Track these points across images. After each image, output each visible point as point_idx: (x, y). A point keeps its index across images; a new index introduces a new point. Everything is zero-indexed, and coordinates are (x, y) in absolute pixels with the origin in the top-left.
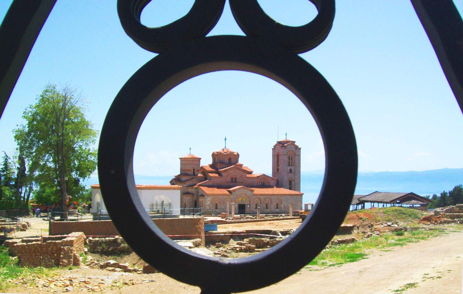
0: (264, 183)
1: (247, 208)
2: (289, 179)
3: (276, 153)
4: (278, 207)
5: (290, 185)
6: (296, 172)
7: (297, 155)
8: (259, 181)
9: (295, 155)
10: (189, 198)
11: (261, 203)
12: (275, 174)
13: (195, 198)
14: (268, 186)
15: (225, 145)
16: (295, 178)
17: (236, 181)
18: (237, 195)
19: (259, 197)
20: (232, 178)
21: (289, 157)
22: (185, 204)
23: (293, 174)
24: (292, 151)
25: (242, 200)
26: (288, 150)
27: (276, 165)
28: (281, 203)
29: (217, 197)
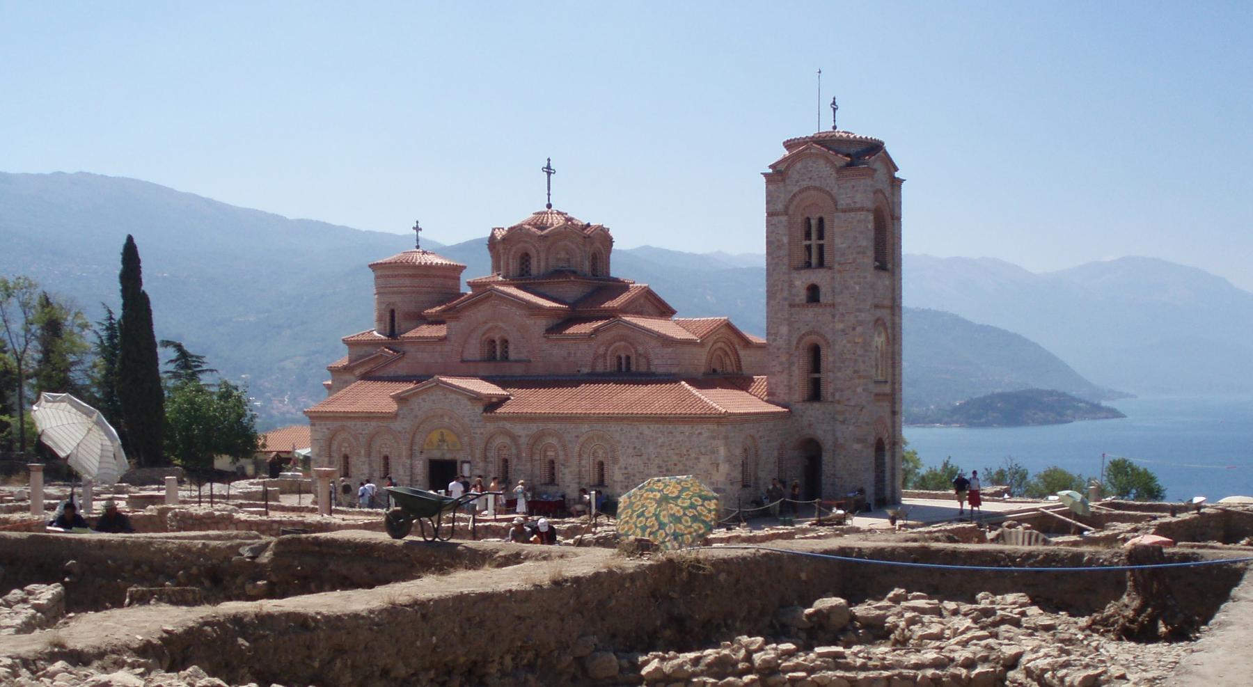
0: (628, 358)
2: (804, 335)
6: (839, 300)
7: (844, 211)
8: (601, 351)
11: (519, 457)
14: (641, 374)
15: (549, 195)
17: (505, 358)
18: (416, 416)
19: (508, 425)
21: (808, 219)
23: (828, 310)
24: (815, 188)
25: (442, 440)
26: (796, 189)
29: (343, 428)
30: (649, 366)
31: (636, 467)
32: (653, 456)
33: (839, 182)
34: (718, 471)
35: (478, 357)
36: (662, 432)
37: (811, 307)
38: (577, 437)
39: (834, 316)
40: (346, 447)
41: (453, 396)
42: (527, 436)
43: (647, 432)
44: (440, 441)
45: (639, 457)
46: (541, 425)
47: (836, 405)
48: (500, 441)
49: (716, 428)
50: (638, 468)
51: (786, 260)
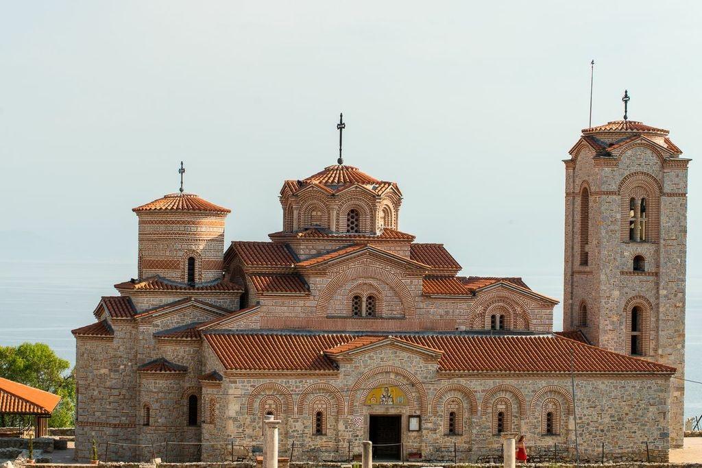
1: (409, 431)
3: (578, 182)
4: (557, 427)
5: (634, 328)
6: (662, 270)
8: (480, 309)
9: (662, 193)
10: (162, 383)
11: (473, 410)
12: (577, 277)
13: (188, 383)
15: (341, 150)
16: (657, 298)
17: (372, 313)
18: (362, 374)
19: (463, 381)
20: (357, 298)
22: (148, 409)
23: (651, 278)
26: (627, 173)
27: (578, 238)
28: (569, 412)
30: (527, 325)
31: (590, 417)
32: (606, 408)
33: (665, 171)
34: (664, 419)
35: (345, 313)
36: (616, 387)
37: (638, 275)
38: (533, 391)
39: (657, 284)
40: (270, 405)
41: (405, 355)
42: (483, 391)
43: (602, 387)
44: (384, 397)
45: (592, 409)
46: (498, 381)
47: (660, 359)
48: (449, 396)
49: (663, 382)
50: (592, 418)
51: (618, 235)
